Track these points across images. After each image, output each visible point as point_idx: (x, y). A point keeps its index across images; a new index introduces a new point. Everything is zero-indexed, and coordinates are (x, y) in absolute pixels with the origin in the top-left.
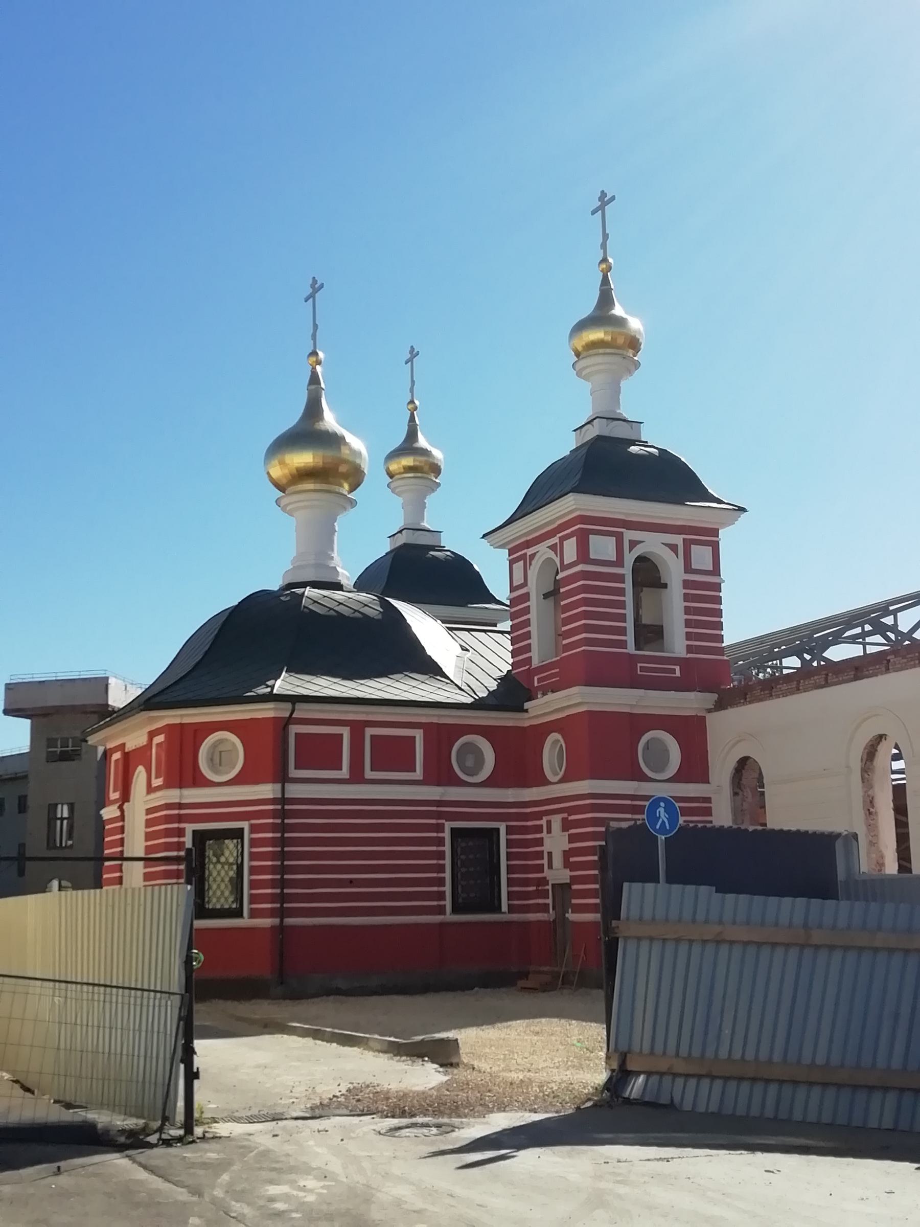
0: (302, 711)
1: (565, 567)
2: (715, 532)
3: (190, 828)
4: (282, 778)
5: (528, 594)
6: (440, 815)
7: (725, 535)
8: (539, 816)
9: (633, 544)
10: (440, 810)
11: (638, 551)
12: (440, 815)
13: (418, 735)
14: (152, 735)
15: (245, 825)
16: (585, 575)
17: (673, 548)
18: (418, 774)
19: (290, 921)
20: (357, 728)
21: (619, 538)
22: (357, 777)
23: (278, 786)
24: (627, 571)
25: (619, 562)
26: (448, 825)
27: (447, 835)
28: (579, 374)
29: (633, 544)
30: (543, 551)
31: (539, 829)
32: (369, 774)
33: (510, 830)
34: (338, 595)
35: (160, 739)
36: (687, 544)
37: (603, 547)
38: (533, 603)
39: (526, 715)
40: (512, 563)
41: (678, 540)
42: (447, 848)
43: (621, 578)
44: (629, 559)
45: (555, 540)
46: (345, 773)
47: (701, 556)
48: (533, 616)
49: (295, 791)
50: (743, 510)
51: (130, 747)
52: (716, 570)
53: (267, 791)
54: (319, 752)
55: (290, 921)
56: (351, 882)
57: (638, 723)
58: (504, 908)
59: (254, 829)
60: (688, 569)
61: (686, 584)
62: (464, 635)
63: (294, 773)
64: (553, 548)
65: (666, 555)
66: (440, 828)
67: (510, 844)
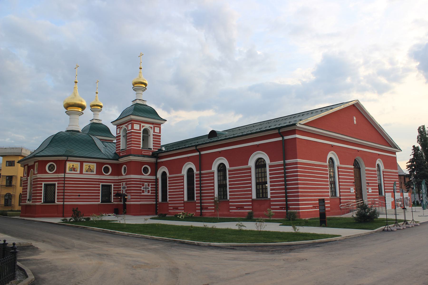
0: (70, 158)
1: (128, 130)
2: (160, 125)
3: (43, 183)
5: (120, 136)
7: (162, 126)
8: (120, 182)
9: (143, 126)
10: (99, 180)
11: (144, 128)
13: (95, 164)
14: (35, 162)
15: (56, 183)
17: (151, 128)
18: (95, 173)
19: (65, 203)
21: (140, 125)
23: (63, 174)
24: (142, 132)
25: (140, 130)
26: (101, 184)
27: (101, 186)
28: (134, 90)
29: (143, 126)
30: (124, 126)
31: (120, 185)
33: (114, 185)
34: (79, 134)
35: (37, 164)
36: (154, 127)
37: (136, 127)
38: (121, 137)
39: (118, 161)
40: (117, 128)
42: (101, 189)
43: (140, 133)
44: (142, 129)
45: (127, 124)
46: (78, 172)
47: (157, 130)
48: (121, 140)
50: (166, 121)
51: (29, 165)
52: (160, 133)
55: (65, 203)
56: (79, 196)
57: (143, 163)
58: (112, 201)
59: (58, 184)
60: (154, 132)
61: (154, 135)
62: (106, 143)
64: (126, 126)
65: (150, 129)
66: (99, 184)
67: (114, 188)
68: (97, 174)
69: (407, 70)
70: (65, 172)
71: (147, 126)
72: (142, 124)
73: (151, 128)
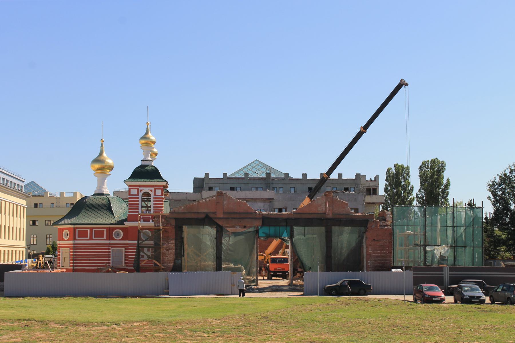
4: (74, 239)
6: (109, 246)
9: (141, 190)
10: (110, 246)
11: (143, 192)
12: (109, 246)
13: (105, 230)
16: (130, 198)
17: (151, 191)
18: (105, 238)
20: (91, 229)
21: (138, 189)
22: (91, 239)
24: (140, 196)
25: (138, 194)
26: (111, 248)
29: (141, 190)
32: (94, 238)
33: (125, 249)
36: (155, 190)
41: (152, 189)
43: (138, 198)
44: (140, 194)
46: (88, 238)
49: (76, 242)
53: (71, 242)
54: (83, 234)
60: (155, 195)
63: (77, 238)
66: (109, 249)
68: (106, 240)
69: (101, 183)
70: (74, 239)
71: (146, 190)
72: (140, 189)
73: (151, 191)
